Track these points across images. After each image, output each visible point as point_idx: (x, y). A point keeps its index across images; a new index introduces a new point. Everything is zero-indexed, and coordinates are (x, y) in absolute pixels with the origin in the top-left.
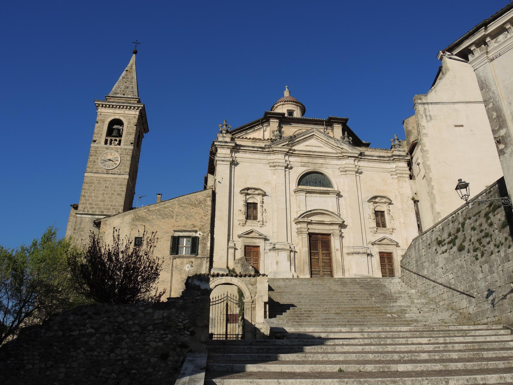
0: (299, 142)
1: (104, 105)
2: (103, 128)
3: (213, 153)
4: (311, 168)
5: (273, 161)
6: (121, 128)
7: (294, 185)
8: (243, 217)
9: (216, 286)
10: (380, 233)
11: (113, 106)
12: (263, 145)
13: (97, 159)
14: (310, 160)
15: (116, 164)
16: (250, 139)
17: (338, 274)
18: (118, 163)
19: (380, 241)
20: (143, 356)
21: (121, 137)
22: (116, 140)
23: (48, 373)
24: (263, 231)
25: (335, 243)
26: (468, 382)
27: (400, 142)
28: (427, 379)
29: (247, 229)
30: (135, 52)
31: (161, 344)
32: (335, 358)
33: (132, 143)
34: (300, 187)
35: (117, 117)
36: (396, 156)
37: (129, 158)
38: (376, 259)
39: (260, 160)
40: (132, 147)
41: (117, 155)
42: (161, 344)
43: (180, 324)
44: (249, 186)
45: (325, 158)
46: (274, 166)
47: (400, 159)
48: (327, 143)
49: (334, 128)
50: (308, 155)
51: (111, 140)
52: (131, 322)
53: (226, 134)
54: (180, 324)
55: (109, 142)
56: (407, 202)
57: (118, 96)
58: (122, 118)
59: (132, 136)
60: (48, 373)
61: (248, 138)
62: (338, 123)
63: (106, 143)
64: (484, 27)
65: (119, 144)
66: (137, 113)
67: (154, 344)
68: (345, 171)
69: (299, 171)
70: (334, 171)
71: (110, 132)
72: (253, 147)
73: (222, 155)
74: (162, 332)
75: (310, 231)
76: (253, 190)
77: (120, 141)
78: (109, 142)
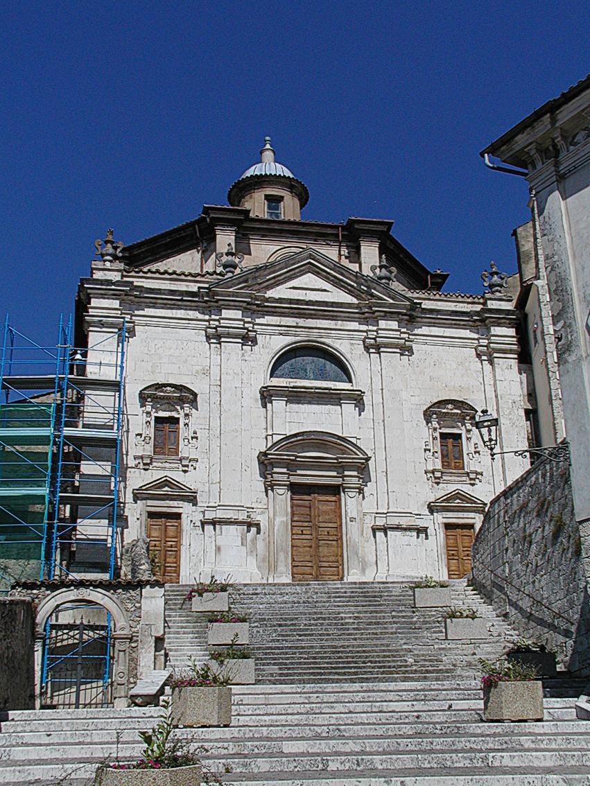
0: (277, 283)
3: (82, 306)
4: (301, 337)
5: (217, 323)
7: (261, 378)
8: (149, 450)
10: (448, 482)
12: (194, 288)
14: (301, 322)
16: (166, 272)
17: (351, 572)
19: (447, 500)
24: (189, 480)
25: (350, 503)
26: (358, 765)
27: (502, 279)
28: (295, 760)
29: (154, 475)
32: (203, 734)
34: (276, 382)
36: (491, 311)
38: (437, 538)
39: (187, 322)
44: (162, 381)
45: (332, 316)
46: (216, 337)
47: (499, 318)
48: (337, 283)
49: (362, 244)
50: (298, 309)
53: (110, 261)
56: (510, 414)
61: (162, 271)
62: (371, 235)
64: (548, 115)
68: (373, 347)
69: (273, 343)
70: (352, 344)
72: (172, 292)
73: (99, 312)
75: (294, 479)
76: (169, 388)
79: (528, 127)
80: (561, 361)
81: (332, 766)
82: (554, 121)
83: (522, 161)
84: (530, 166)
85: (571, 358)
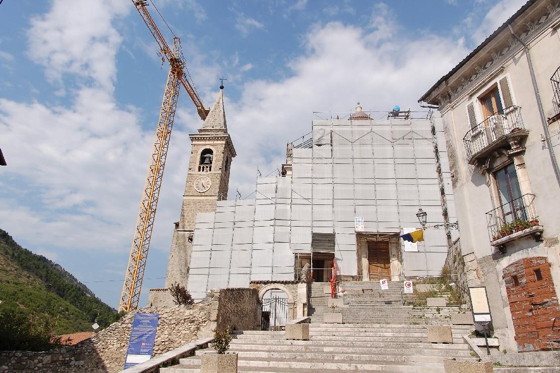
1: (197, 138)
2: (197, 157)
6: (212, 156)
9: (267, 291)
11: (204, 138)
13: (193, 184)
15: (207, 187)
18: (209, 186)
20: (177, 339)
21: (211, 163)
22: (207, 167)
23: (121, 350)
30: (222, 88)
31: (188, 332)
33: (220, 169)
35: (208, 147)
37: (218, 181)
40: (220, 172)
41: (209, 179)
42: (188, 332)
43: (200, 319)
51: (203, 168)
52: (171, 318)
54: (200, 319)
55: (201, 169)
57: (208, 128)
58: (211, 148)
59: (220, 162)
60: (121, 350)
63: (199, 170)
65: (210, 170)
66: (224, 142)
67: (184, 332)
71: (203, 160)
74: (190, 324)
77: (210, 168)
78: (201, 169)
79: (436, 88)
80: (454, 185)
81: (336, 358)
82: (447, 84)
83: (435, 102)
84: (439, 104)
85: (458, 185)
